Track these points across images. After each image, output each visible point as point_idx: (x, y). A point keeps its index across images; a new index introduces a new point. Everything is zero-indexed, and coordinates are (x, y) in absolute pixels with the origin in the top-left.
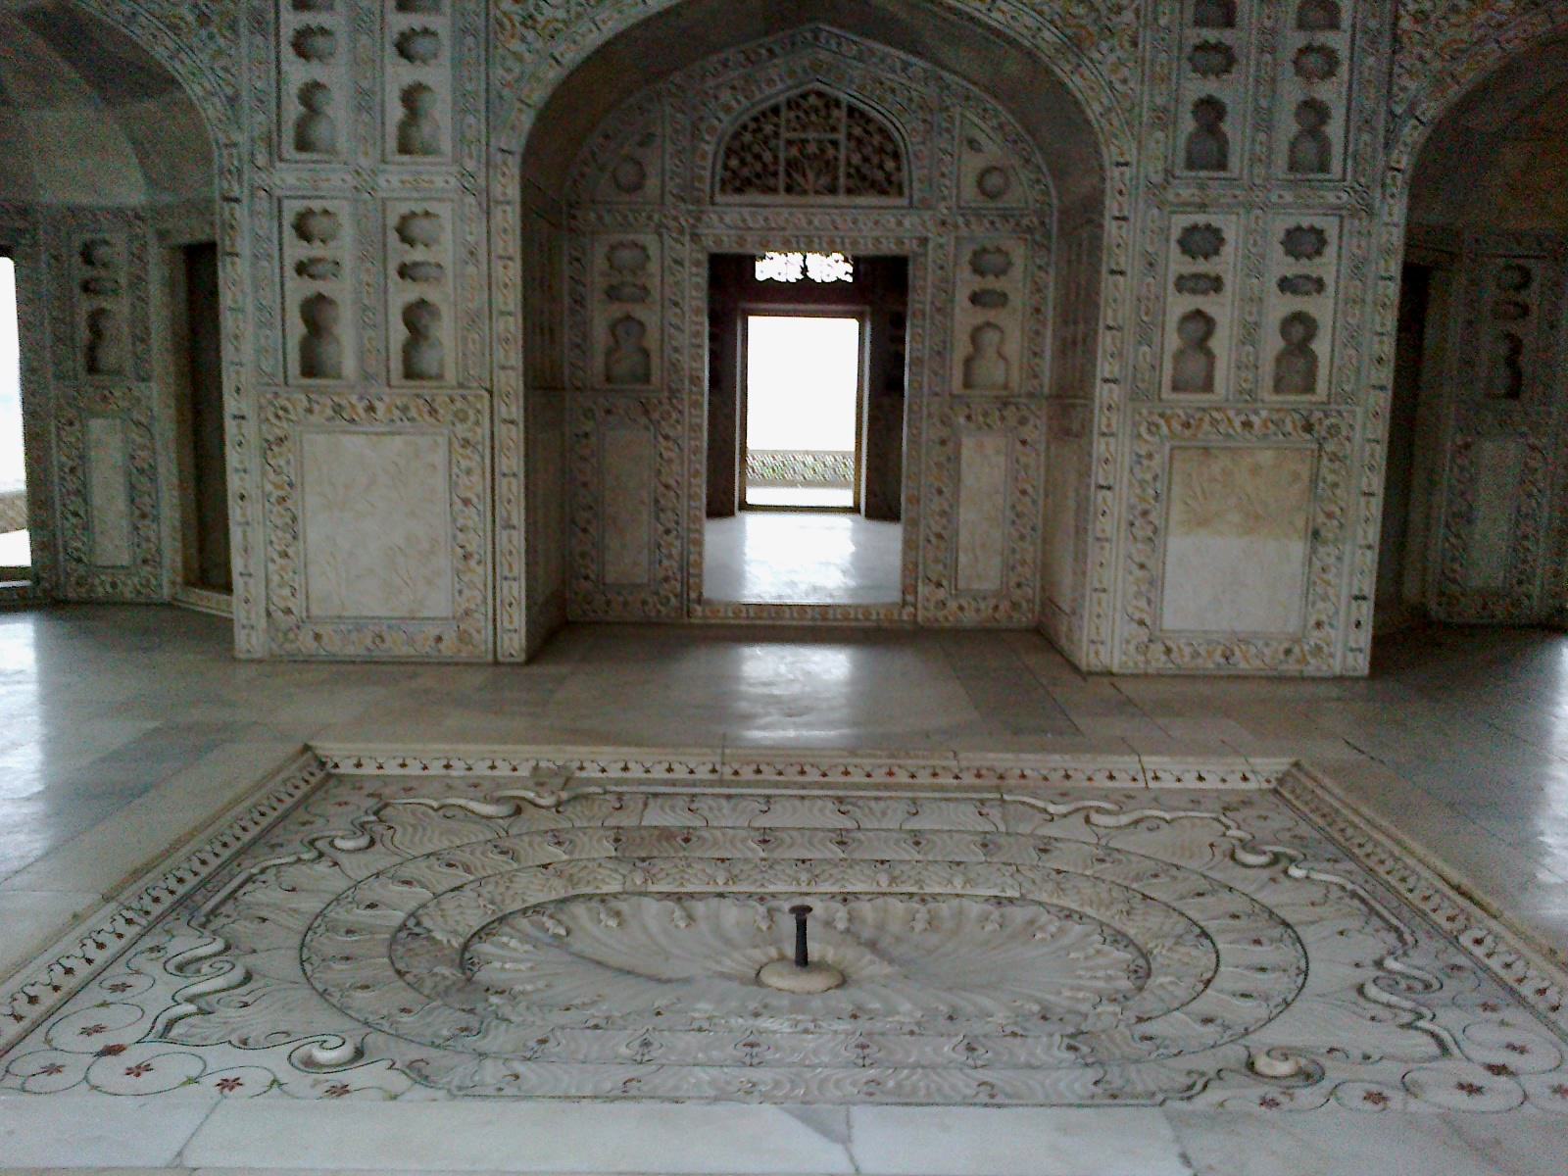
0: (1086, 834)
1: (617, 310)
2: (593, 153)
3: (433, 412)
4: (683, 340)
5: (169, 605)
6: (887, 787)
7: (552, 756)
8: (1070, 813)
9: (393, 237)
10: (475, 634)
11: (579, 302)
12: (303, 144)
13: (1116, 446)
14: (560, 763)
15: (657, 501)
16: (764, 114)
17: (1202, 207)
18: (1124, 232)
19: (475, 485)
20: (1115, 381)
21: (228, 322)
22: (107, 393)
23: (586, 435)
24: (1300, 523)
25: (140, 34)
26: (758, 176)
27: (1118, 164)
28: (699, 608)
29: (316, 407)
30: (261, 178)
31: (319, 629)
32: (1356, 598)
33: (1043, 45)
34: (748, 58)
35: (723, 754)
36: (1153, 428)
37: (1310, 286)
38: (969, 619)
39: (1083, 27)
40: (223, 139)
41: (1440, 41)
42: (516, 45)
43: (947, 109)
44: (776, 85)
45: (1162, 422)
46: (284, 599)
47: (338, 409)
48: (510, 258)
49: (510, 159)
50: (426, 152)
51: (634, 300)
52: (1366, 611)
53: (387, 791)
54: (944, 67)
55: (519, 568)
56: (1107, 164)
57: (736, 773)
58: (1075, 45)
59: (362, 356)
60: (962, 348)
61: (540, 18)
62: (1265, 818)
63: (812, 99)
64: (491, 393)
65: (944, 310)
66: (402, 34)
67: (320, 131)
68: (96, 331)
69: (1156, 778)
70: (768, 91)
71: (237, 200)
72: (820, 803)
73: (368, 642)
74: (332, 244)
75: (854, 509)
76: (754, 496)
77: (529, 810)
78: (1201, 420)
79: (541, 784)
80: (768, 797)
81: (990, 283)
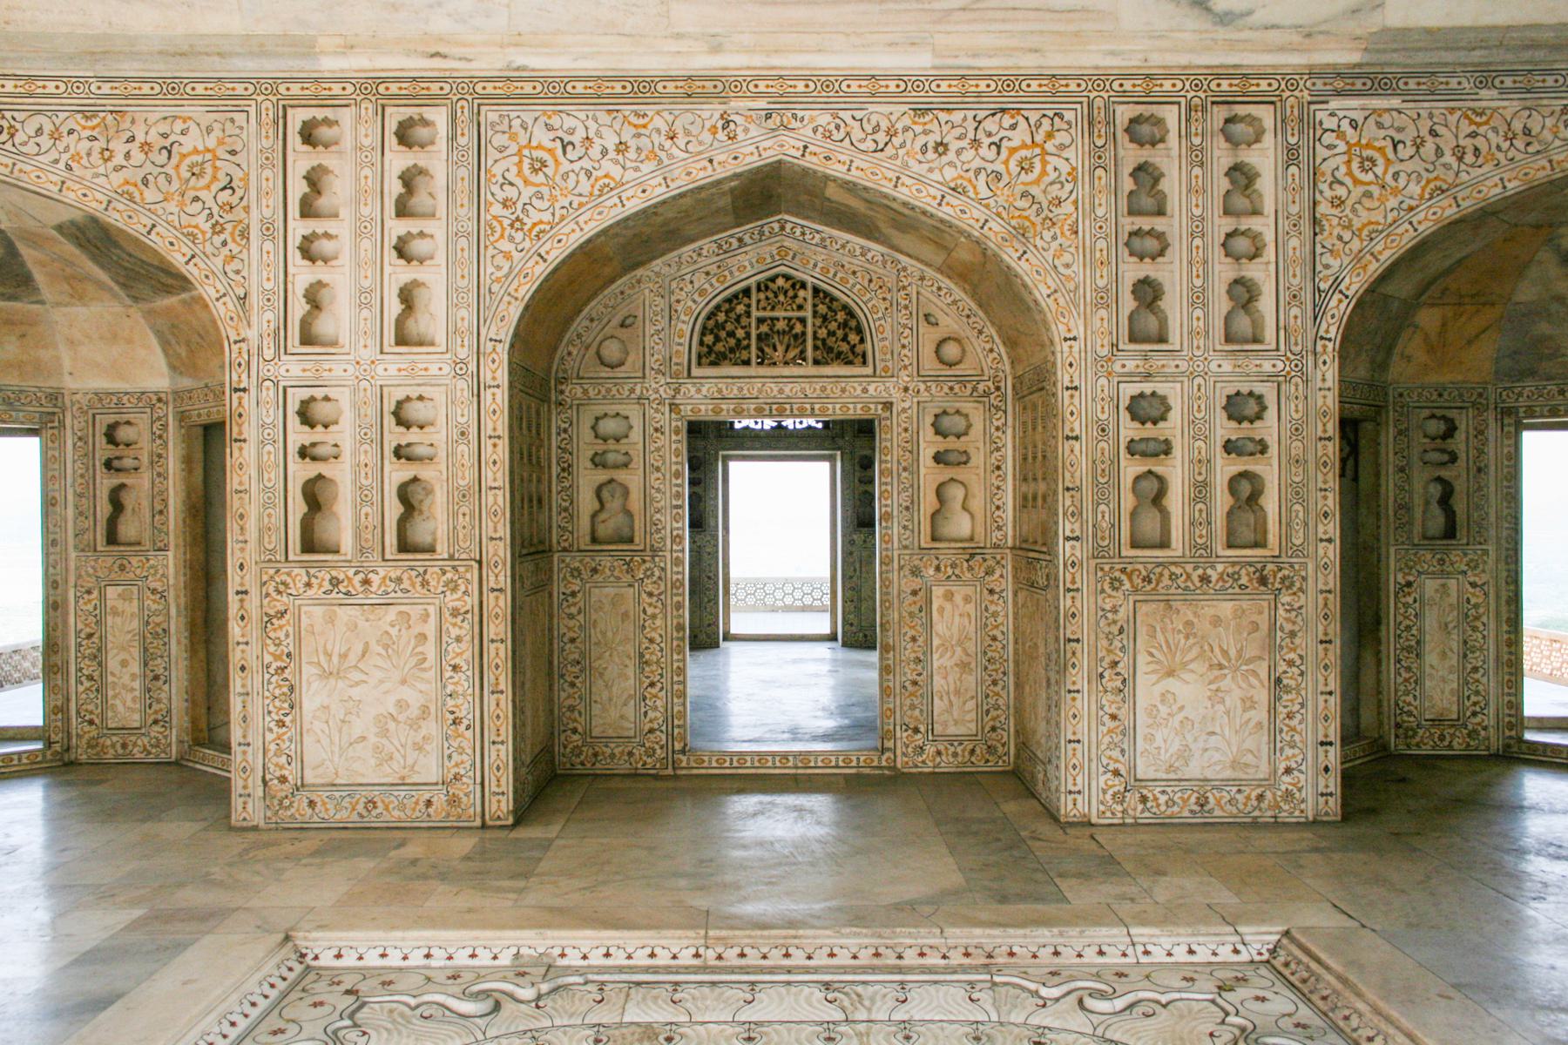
0: (1079, 1021)
1: (602, 476)
2: (579, 336)
3: (425, 583)
4: (664, 501)
5: (177, 763)
6: (874, 969)
7: (535, 942)
8: (1064, 996)
9: (389, 421)
10: (465, 799)
11: (567, 469)
12: (307, 339)
13: (1083, 602)
14: (541, 950)
15: (641, 655)
16: (735, 296)
17: (1148, 376)
18: (1076, 401)
19: (462, 653)
20: (1077, 539)
21: (234, 503)
23: (573, 594)
24: (1264, 675)
25: (157, 242)
26: (732, 350)
27: (1066, 339)
28: (684, 758)
30: (270, 370)
31: (314, 797)
32: (1322, 744)
33: (990, 235)
34: (720, 247)
35: (706, 937)
36: (1115, 584)
37: (1251, 447)
38: (947, 764)
39: (1027, 218)
41: (1357, 223)
42: (505, 245)
43: (904, 288)
44: (746, 267)
45: (1123, 577)
46: (282, 768)
47: (335, 582)
49: (499, 347)
50: (421, 344)
51: (616, 467)
52: (1333, 756)
53: (363, 987)
54: (902, 252)
55: (507, 732)
56: (1057, 339)
57: (720, 957)
58: (1022, 233)
60: (928, 502)
61: (526, 220)
62: (1263, 999)
63: (780, 282)
64: (480, 562)
65: (912, 469)
66: (399, 238)
67: (324, 326)
68: (117, 505)
69: (1146, 953)
70: (739, 276)
71: (244, 390)
72: (806, 990)
73: (360, 808)
74: (331, 428)
75: (832, 637)
76: (739, 623)
77: (508, 1007)
78: (1161, 575)
79: (523, 974)
80: (753, 983)
81: (951, 443)
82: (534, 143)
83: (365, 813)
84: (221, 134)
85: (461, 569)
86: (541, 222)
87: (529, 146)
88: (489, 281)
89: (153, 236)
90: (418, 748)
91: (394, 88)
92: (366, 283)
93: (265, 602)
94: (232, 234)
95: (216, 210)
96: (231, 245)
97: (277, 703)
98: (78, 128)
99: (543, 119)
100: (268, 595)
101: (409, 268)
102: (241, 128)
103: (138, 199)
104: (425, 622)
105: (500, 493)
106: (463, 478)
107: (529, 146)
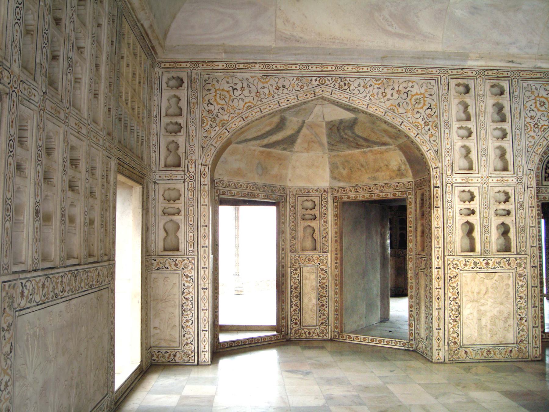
3: (509, 264)
22: (311, 258)
29: (467, 263)
31: (467, 350)
40: (434, 166)
42: (532, 134)
46: (455, 338)
47: (476, 264)
48: (533, 207)
49: (532, 172)
59: (482, 242)
61: (539, 124)
71: (438, 187)
73: (485, 354)
82: (540, 95)
83: (486, 355)
84: (426, 88)
85: (523, 258)
86: (545, 125)
87: (538, 96)
88: (527, 147)
89: (402, 126)
90: (507, 330)
91: (490, 73)
92: (484, 147)
93: (449, 272)
94: (432, 126)
95: (425, 117)
96: (431, 130)
97: (453, 312)
98: (373, 84)
99: (543, 87)
100: (450, 269)
101: (498, 141)
102: (434, 86)
103: (396, 112)
104: (509, 279)
105: (534, 229)
106: (522, 223)
107: (538, 96)
